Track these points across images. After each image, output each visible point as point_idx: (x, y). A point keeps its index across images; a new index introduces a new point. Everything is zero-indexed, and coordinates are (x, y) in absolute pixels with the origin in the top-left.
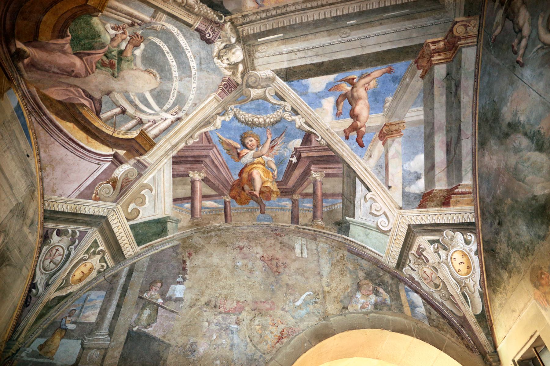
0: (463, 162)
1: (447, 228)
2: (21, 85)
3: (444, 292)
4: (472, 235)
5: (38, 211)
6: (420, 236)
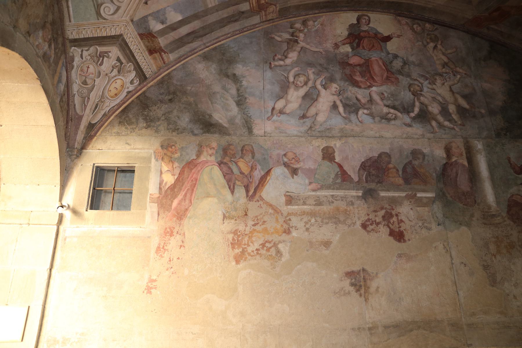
0: (184, 48)
1: (134, 63)
3: (85, 91)
4: (138, 81)
6: (118, 48)
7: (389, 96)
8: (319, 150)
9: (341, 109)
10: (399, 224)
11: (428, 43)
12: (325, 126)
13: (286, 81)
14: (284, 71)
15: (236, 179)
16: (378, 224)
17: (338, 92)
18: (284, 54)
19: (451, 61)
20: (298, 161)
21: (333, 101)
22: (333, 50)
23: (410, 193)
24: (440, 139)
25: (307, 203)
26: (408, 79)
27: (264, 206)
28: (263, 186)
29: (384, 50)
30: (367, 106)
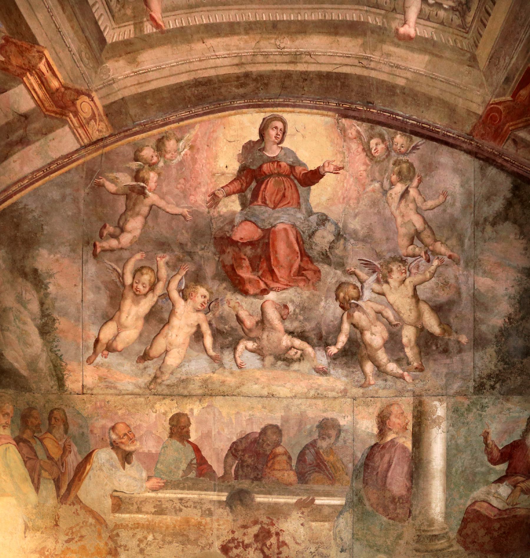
7: (297, 311)
8: (165, 421)
9: (208, 341)
10: (278, 548)
11: (392, 184)
12: (179, 376)
13: (119, 284)
14: (118, 261)
15: (42, 467)
16: (246, 547)
17: (206, 306)
18: (119, 223)
19: (429, 226)
20: (132, 440)
21: (196, 324)
22: (207, 210)
23: (304, 498)
24: (372, 399)
25: (144, 509)
26: (339, 272)
27: (82, 512)
28: (80, 480)
29: (303, 206)
30: (253, 335)
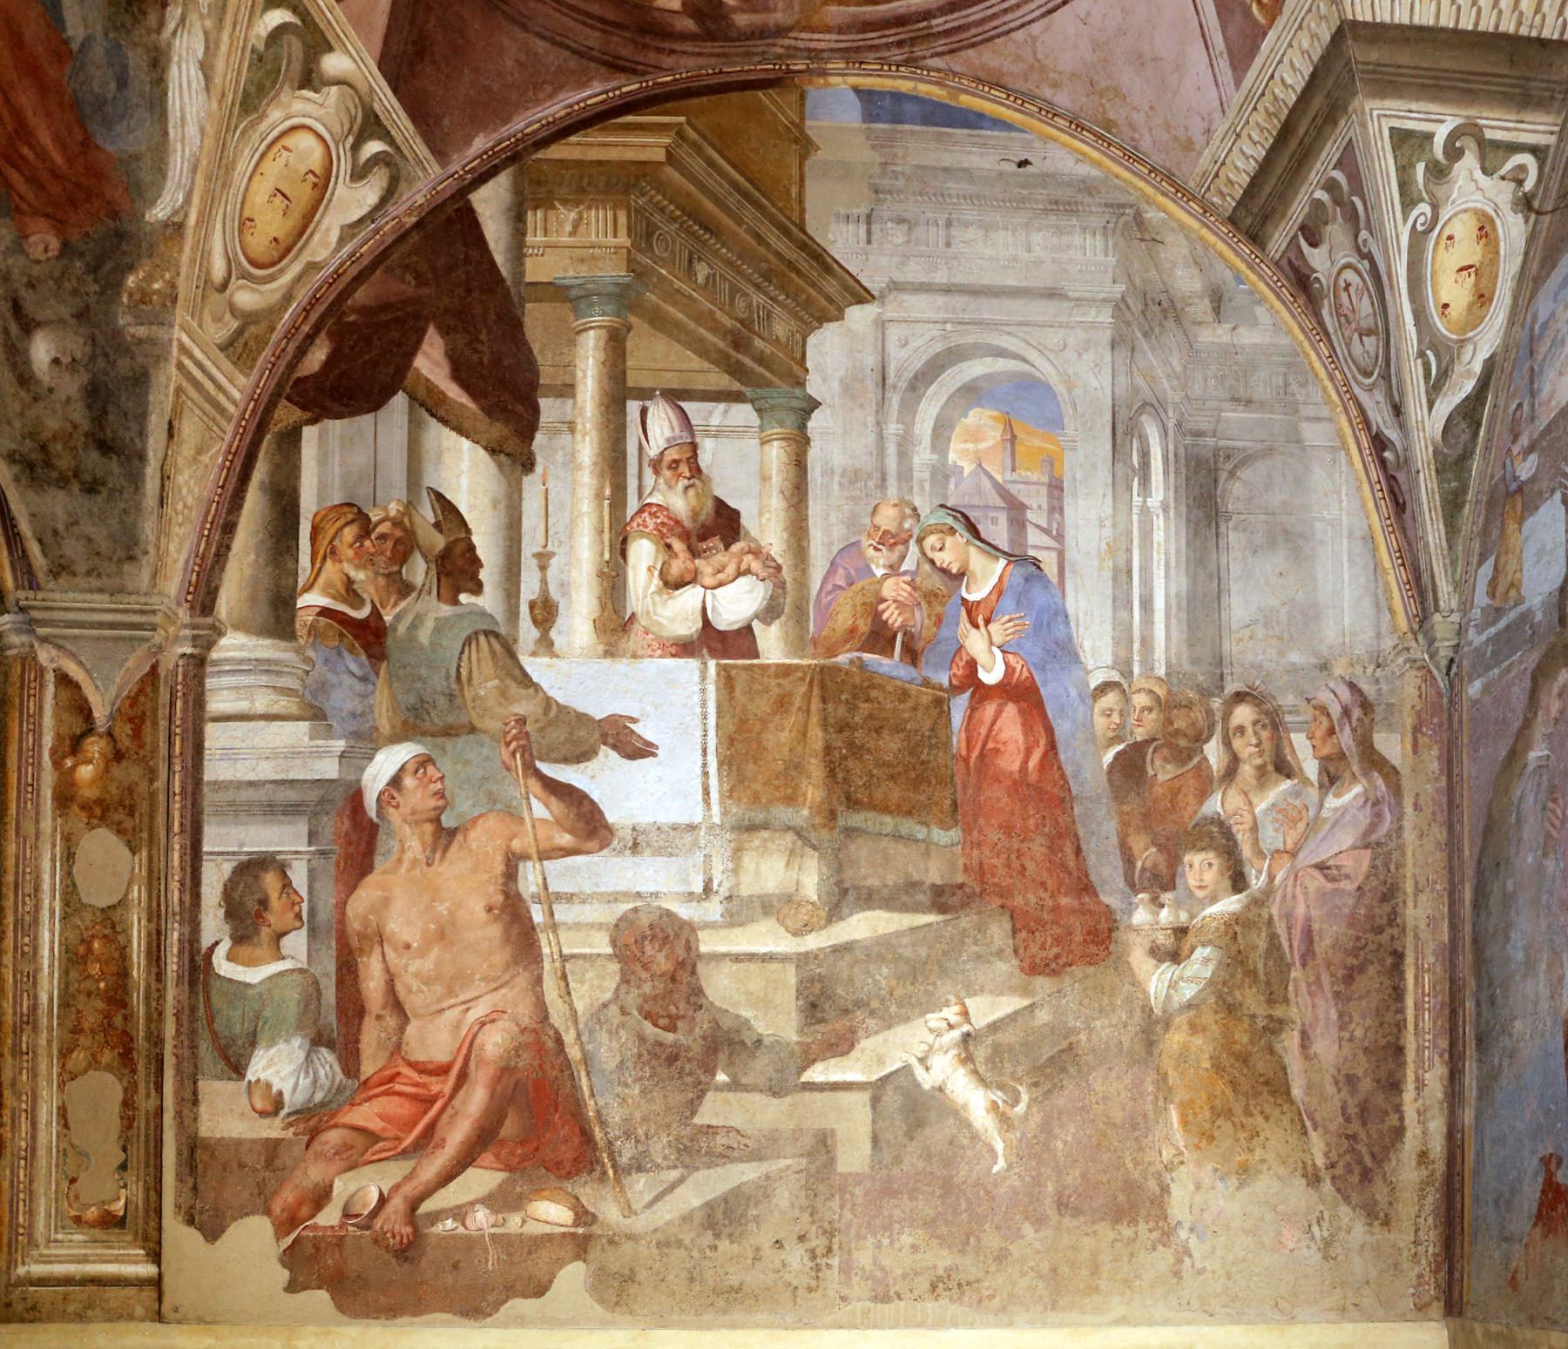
2: (813, 45)
5: (1207, 246)
